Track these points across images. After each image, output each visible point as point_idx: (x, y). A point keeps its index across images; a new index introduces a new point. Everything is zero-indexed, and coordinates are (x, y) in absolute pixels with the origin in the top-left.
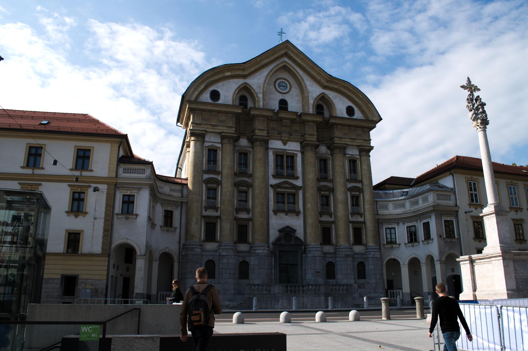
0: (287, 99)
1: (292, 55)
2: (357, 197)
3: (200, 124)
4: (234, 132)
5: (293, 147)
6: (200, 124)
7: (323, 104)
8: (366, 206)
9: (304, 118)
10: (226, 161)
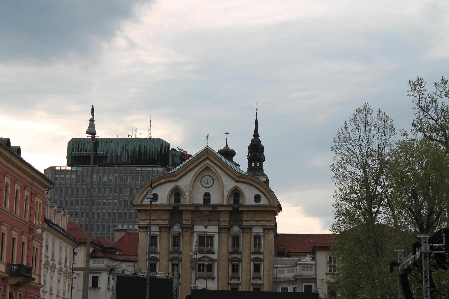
0: (210, 192)
1: (211, 158)
2: (259, 266)
3: (145, 220)
4: (168, 223)
5: (212, 229)
6: (145, 220)
7: (236, 194)
8: (265, 272)
9: (218, 209)
10: (164, 244)
